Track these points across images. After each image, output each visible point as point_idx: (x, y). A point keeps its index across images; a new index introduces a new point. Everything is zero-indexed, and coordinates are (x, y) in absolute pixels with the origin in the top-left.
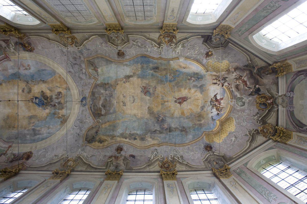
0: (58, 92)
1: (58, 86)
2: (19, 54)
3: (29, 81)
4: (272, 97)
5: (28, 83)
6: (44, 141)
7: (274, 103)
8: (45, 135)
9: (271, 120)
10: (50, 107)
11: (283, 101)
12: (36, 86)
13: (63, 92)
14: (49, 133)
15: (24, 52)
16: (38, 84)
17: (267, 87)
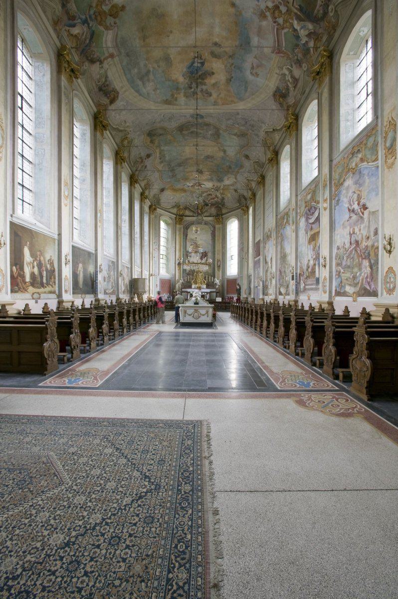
0: (211, 93)
1: (221, 96)
2: (277, 74)
3: (233, 61)
4: (202, 213)
5: (230, 57)
6: (136, 94)
7: (199, 214)
8: (144, 90)
9: (187, 213)
10: (187, 83)
11: (199, 219)
12: (223, 67)
13: (212, 99)
14: (148, 94)
15: (276, 85)
16: (227, 72)
17: (209, 210)
